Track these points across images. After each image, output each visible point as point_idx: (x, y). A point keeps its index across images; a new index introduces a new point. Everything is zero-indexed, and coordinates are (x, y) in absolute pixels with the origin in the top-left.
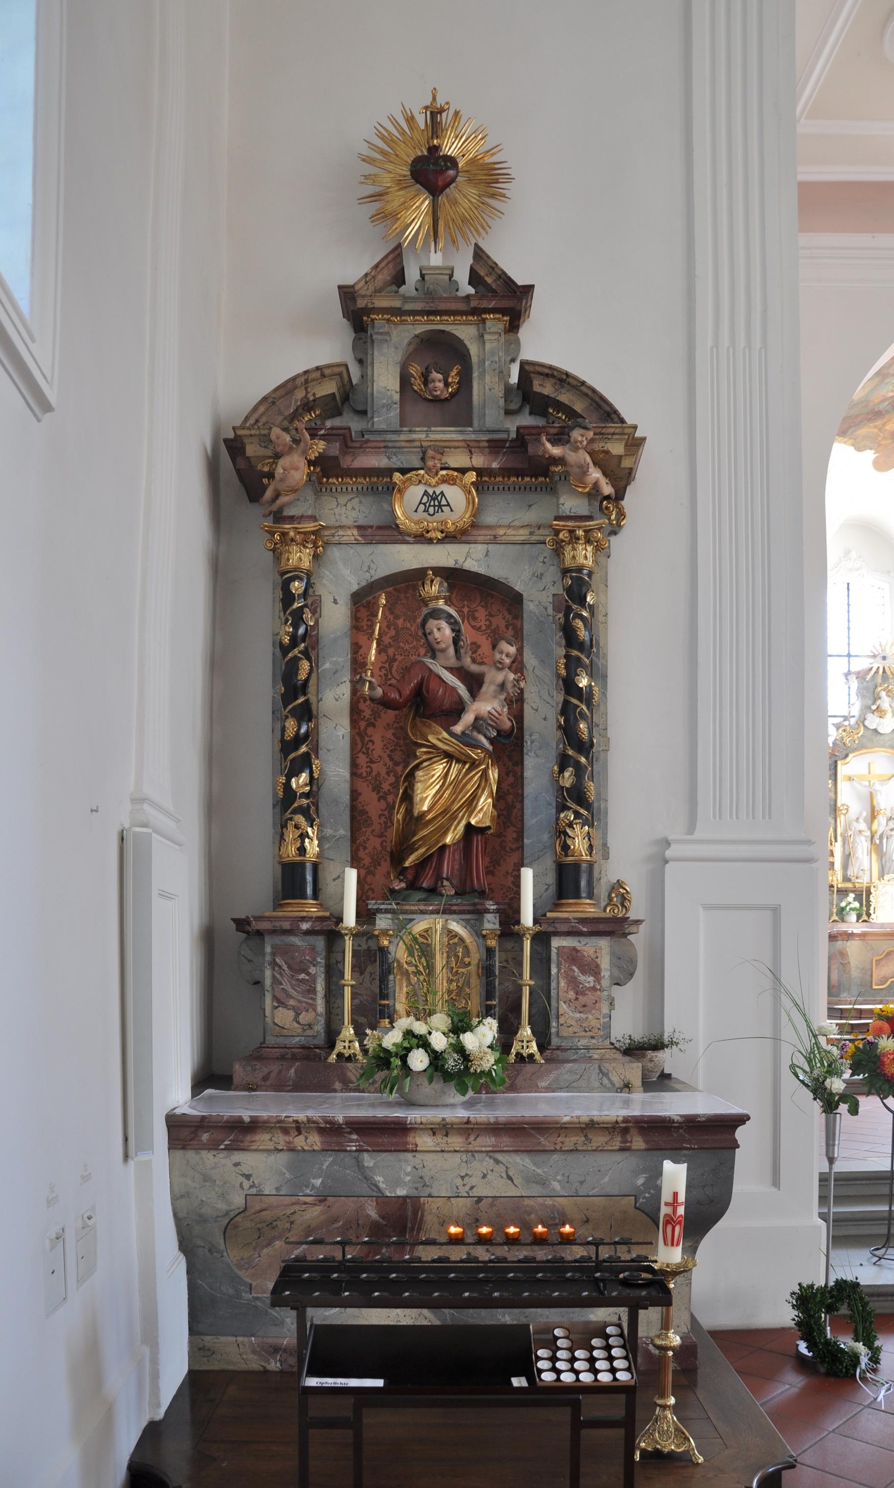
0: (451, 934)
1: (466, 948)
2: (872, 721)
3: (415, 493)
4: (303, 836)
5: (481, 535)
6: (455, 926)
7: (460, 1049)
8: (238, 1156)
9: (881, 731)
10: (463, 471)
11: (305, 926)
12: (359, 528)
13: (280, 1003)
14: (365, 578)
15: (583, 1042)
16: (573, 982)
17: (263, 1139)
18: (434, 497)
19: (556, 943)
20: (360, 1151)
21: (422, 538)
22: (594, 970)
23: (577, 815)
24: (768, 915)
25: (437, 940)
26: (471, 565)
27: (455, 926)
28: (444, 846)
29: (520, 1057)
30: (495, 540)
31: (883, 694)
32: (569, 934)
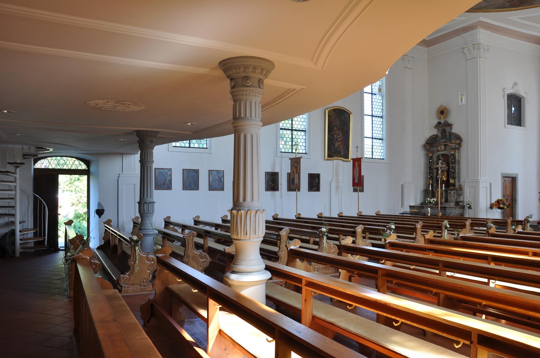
3: (439, 147)
5: (446, 150)
7: (430, 200)
12: (437, 151)
16: (450, 195)
19: (448, 191)
21: (441, 151)
22: (451, 194)
24: (486, 188)
26: (446, 153)
30: (447, 150)
32: (449, 190)
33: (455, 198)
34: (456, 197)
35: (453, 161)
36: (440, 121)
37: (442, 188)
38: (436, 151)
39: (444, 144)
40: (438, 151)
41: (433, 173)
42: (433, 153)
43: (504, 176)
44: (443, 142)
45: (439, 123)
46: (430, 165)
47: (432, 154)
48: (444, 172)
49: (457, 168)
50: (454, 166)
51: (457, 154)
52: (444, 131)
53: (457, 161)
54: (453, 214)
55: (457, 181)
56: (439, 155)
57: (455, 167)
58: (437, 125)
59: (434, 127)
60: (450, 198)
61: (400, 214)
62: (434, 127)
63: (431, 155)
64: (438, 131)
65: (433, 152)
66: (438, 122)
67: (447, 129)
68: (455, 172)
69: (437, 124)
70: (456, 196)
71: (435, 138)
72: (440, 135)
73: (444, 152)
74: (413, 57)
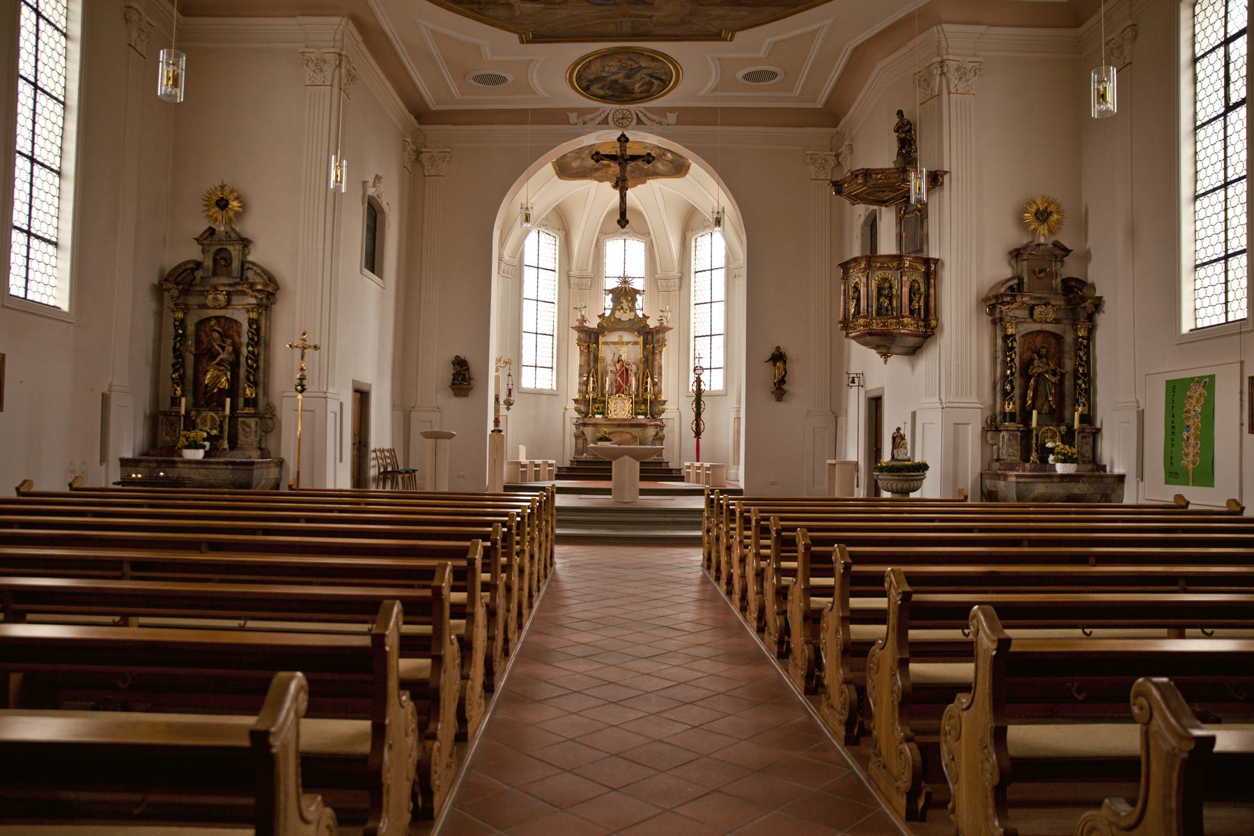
0: (212, 416)
1: (216, 421)
2: (618, 314)
3: (210, 297)
4: (176, 390)
5: (230, 307)
6: (214, 415)
8: (136, 469)
9: (623, 319)
10: (222, 291)
11: (173, 414)
13: (167, 434)
14: (200, 319)
15: (247, 446)
16: (244, 430)
17: (143, 464)
18: (215, 298)
19: (240, 419)
20: (165, 467)
21: (214, 308)
22: (249, 426)
23: (248, 385)
25: (209, 417)
27: (214, 415)
28: (214, 393)
29: (223, 449)
30: (234, 309)
31: (624, 301)
32: (243, 417)
33: (258, 439)
34: (260, 435)
35: (256, 339)
36: (214, 227)
37: (224, 410)
38: (196, 307)
39: (227, 289)
40: (205, 307)
41: (183, 366)
42: (186, 311)
43: (358, 387)
44: (224, 285)
45: (211, 231)
46: (178, 344)
47: (184, 314)
48: (223, 366)
49: (262, 357)
50: (256, 352)
51: (263, 320)
52: (222, 260)
53: (263, 339)
54: (264, 481)
55: (261, 391)
56: (209, 319)
57: (259, 354)
58: (207, 235)
59: (196, 239)
60: (247, 437)
61: (114, 484)
62: (196, 239)
63: (180, 315)
64: (203, 252)
65: (186, 309)
66: (210, 228)
67: (235, 250)
68: (258, 367)
69: (204, 233)
70: (259, 432)
71: (193, 270)
72: (209, 263)
73: (223, 310)
74: (152, 26)
